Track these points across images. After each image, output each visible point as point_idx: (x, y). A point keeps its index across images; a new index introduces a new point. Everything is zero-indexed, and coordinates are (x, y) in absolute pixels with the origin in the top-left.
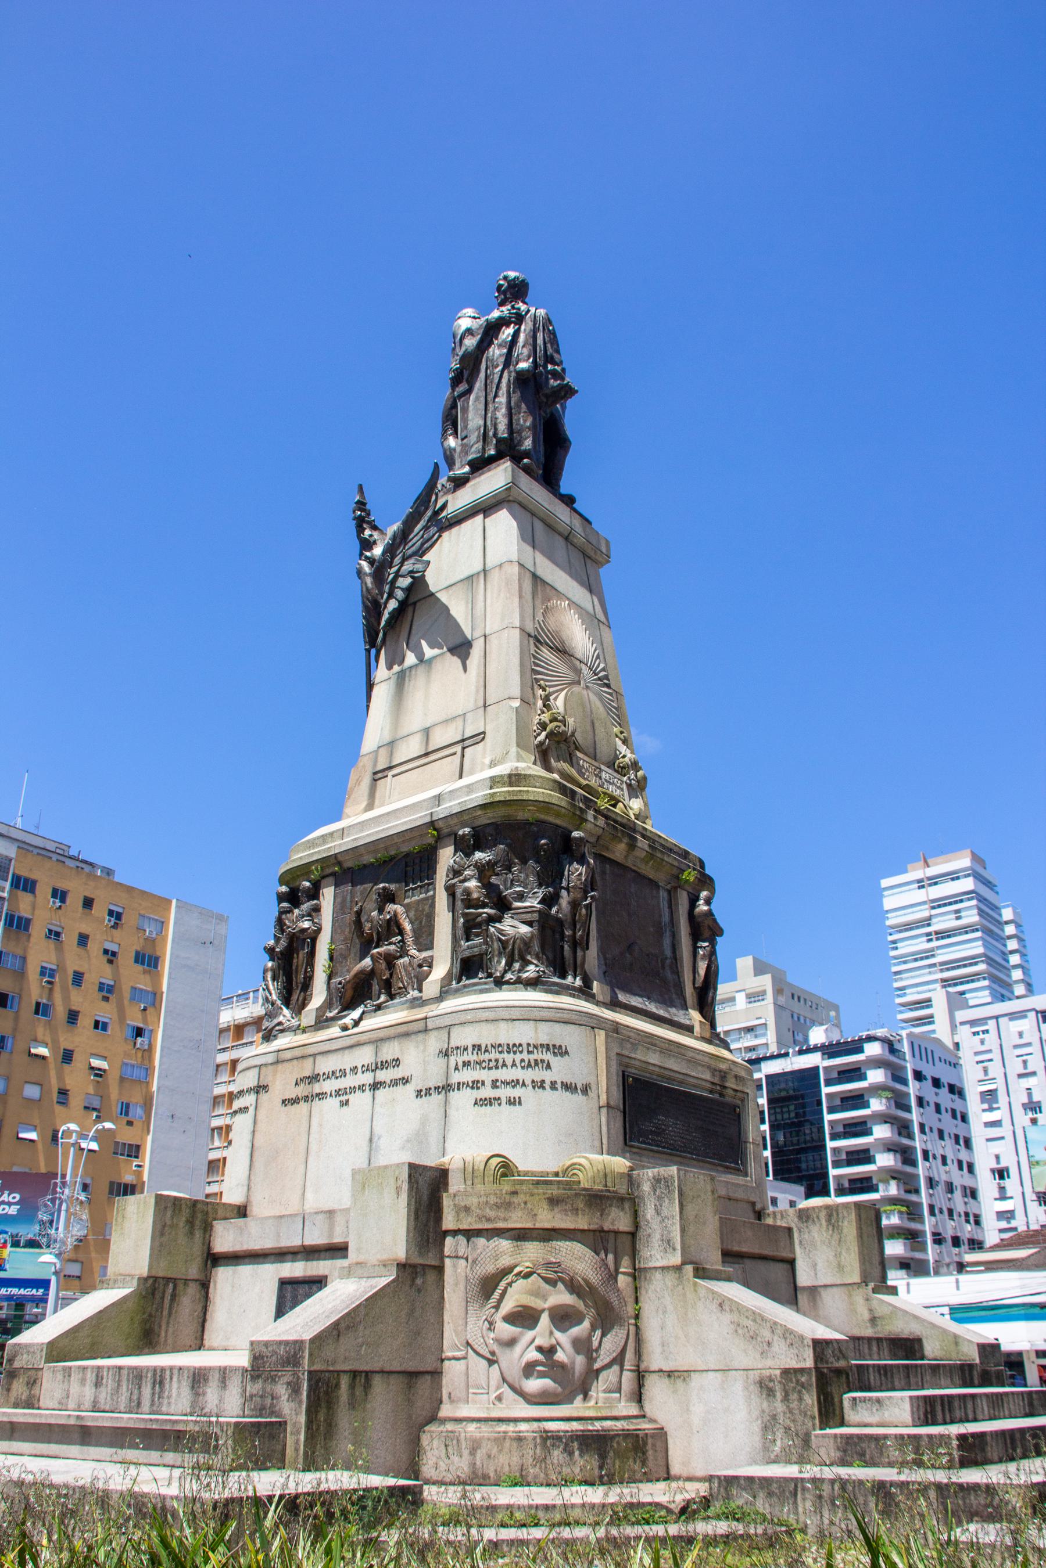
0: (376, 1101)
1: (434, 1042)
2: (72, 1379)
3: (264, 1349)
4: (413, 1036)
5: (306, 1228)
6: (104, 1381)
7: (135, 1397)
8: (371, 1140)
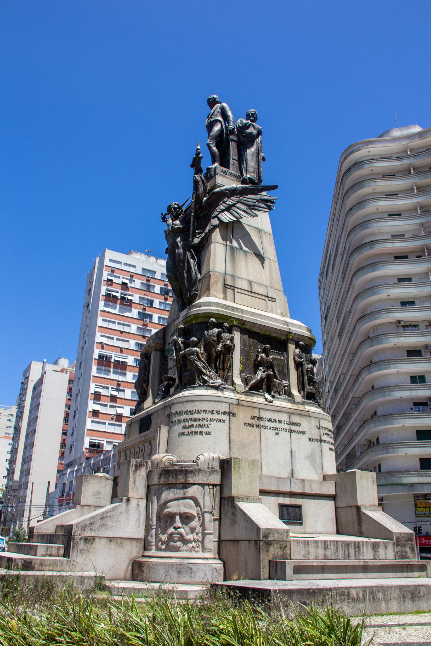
0: (292, 437)
1: (314, 422)
2: (310, 546)
3: (399, 535)
4: (305, 417)
5: (292, 484)
6: (329, 547)
7: (347, 553)
8: (291, 452)
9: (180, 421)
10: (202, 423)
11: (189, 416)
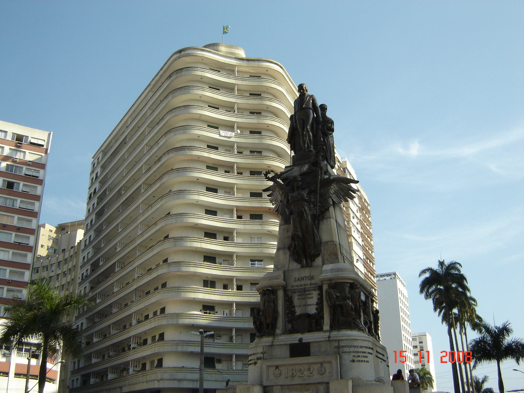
9: (351, 352)
10: (364, 354)
11: (357, 349)
